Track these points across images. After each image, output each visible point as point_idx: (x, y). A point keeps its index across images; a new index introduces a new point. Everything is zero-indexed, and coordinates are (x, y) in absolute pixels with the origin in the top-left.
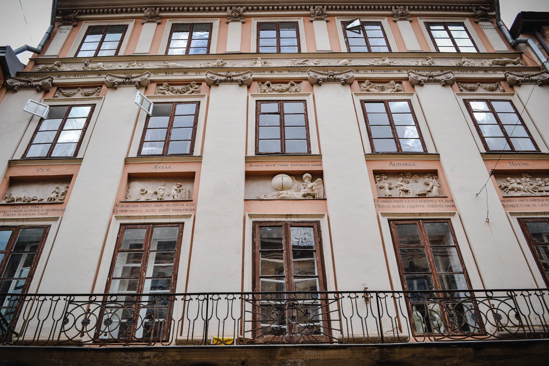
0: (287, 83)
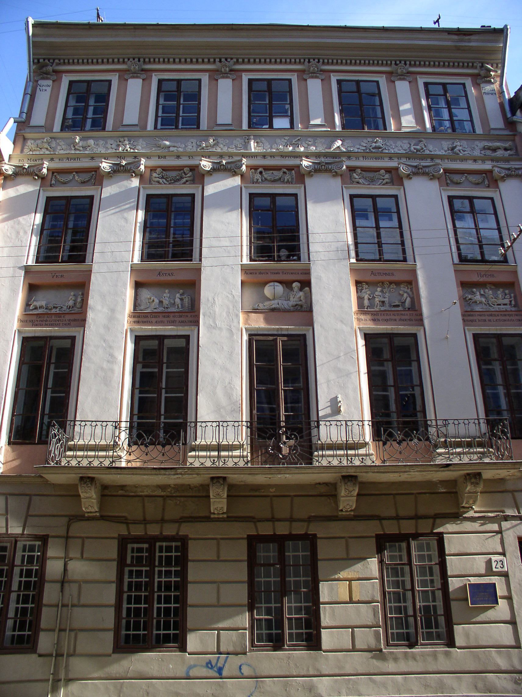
0: (280, 169)
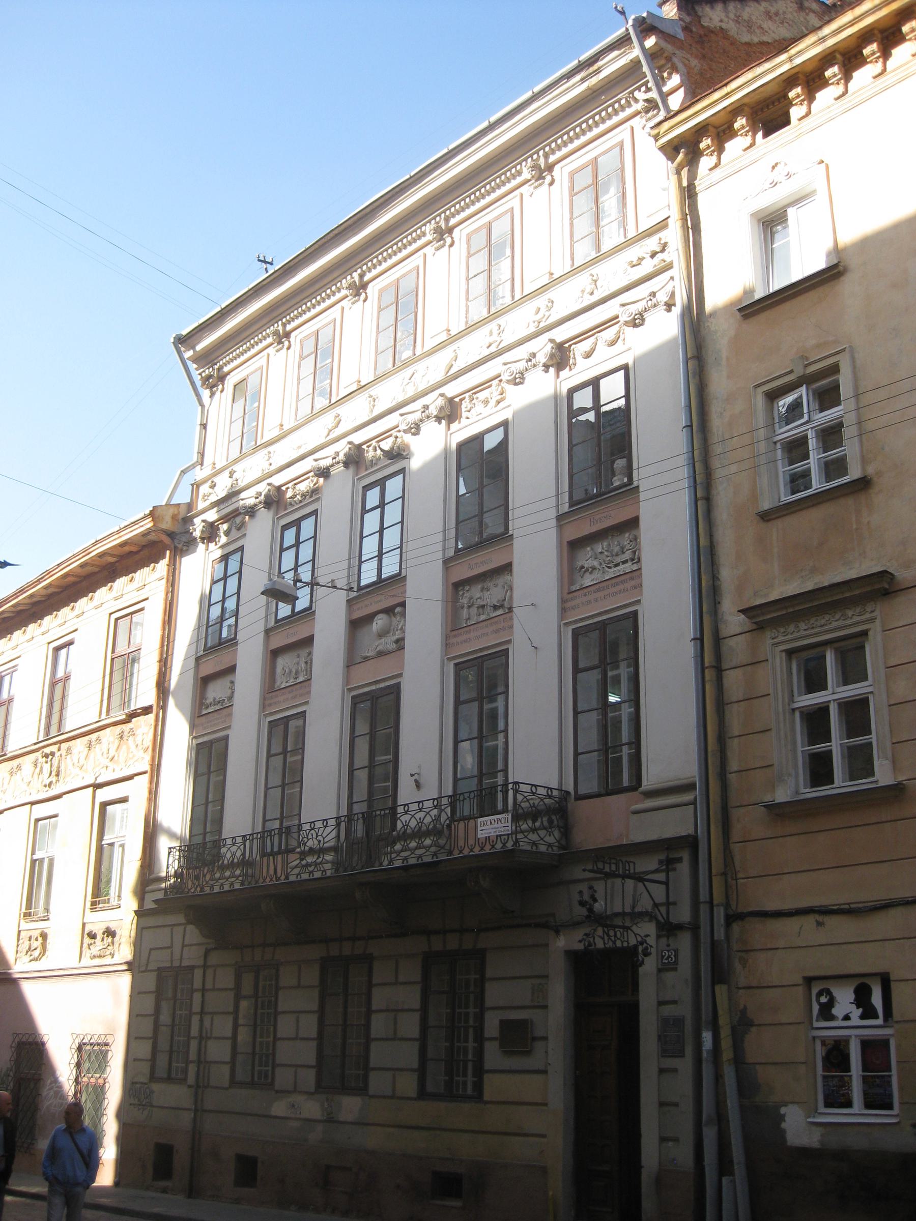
0: (391, 436)
